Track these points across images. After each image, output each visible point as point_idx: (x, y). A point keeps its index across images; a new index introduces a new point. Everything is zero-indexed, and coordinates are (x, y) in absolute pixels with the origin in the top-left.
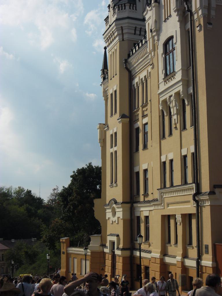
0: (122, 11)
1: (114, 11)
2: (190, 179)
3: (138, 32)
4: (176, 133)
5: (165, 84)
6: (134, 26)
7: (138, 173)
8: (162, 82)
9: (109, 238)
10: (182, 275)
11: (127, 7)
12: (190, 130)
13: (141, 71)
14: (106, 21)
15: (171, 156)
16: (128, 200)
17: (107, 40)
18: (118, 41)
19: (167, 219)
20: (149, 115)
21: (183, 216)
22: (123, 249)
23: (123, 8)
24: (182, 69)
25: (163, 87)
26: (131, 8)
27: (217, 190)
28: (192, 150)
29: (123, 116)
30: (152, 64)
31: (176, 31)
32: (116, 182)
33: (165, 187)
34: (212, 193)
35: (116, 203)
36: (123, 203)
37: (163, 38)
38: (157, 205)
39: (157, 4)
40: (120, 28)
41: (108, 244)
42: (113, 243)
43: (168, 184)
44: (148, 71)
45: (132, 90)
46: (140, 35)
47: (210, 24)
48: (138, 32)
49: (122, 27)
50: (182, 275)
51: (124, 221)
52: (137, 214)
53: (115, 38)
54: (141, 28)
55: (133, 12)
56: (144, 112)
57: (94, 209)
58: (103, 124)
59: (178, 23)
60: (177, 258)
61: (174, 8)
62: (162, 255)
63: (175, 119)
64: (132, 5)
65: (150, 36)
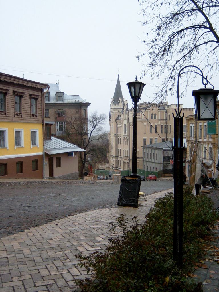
2: (128, 156)
4: (126, 145)
7: (119, 149)
11: (116, 105)
12: (128, 146)
15: (125, 150)
19: (124, 162)
29: (115, 135)
41: (111, 166)
42: (112, 166)
51: (115, 161)
52: (118, 159)
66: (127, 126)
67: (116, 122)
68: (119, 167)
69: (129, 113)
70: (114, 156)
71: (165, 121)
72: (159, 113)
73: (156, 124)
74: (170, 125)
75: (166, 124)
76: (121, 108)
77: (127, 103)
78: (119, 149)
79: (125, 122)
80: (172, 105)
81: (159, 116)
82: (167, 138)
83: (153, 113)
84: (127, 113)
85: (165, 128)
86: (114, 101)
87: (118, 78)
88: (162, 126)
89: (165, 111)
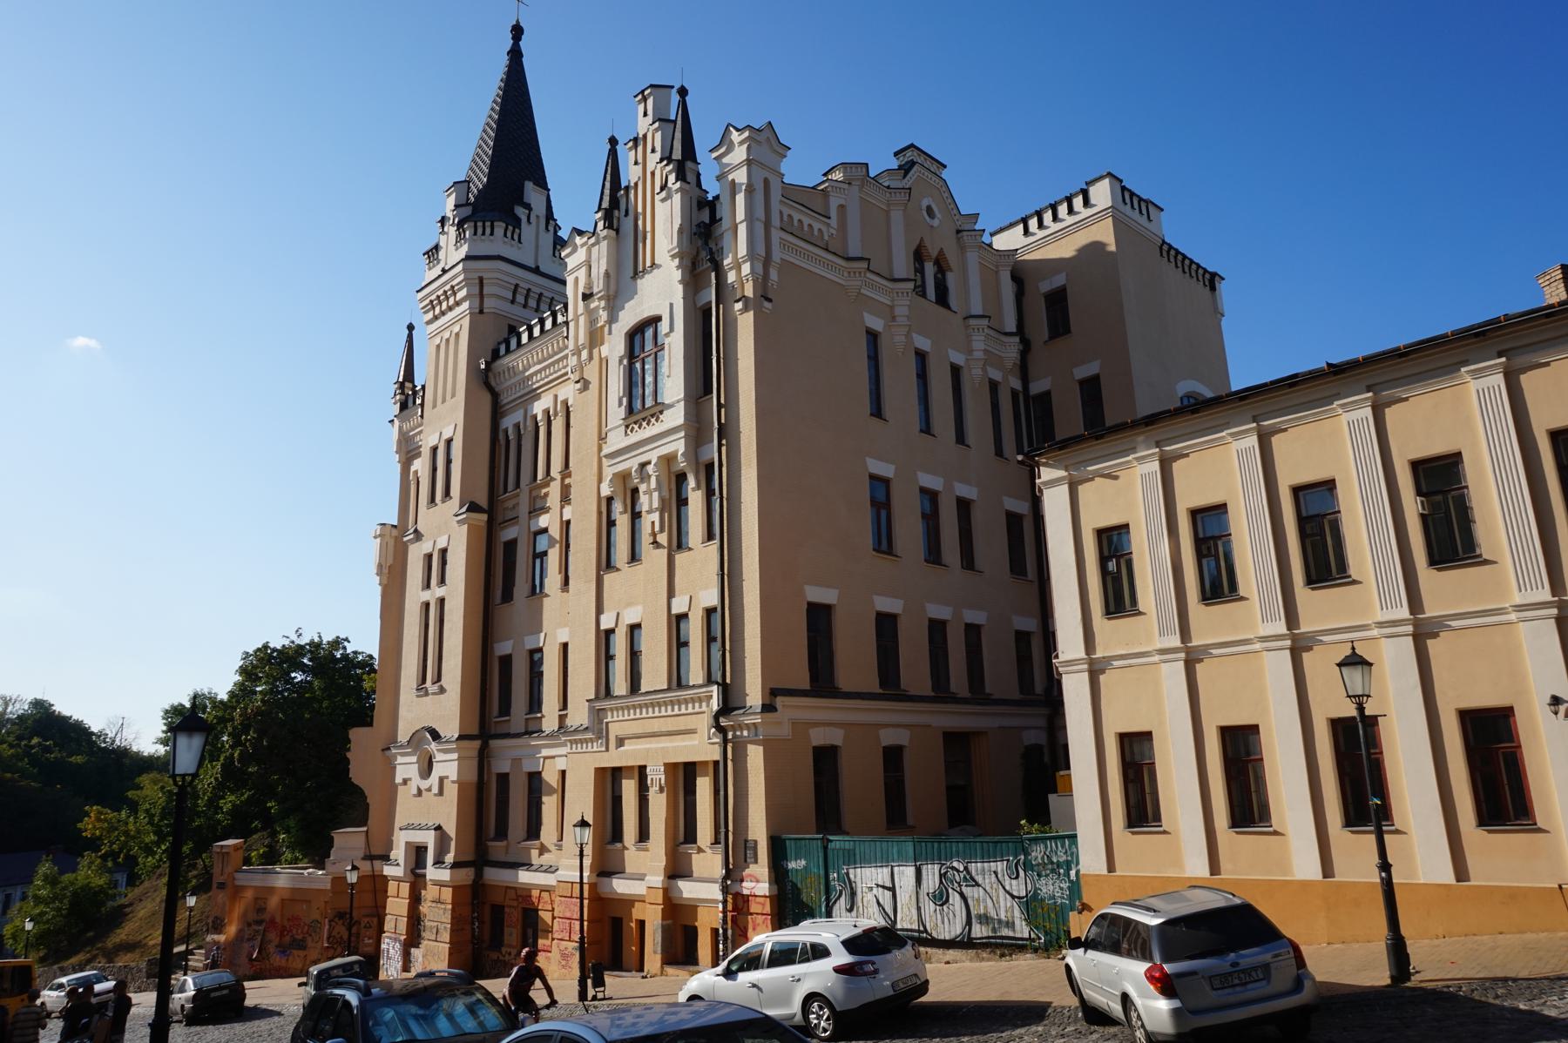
0: (483, 237)
1: (460, 234)
3: (520, 299)
5: (626, 432)
6: (514, 282)
8: (620, 426)
9: (401, 841)
10: (665, 923)
14: (429, 257)
16: (475, 731)
17: (430, 306)
18: (468, 312)
19: (610, 779)
21: (671, 768)
22: (456, 865)
23: (488, 231)
24: (687, 398)
25: (617, 440)
26: (509, 234)
28: (711, 598)
30: (582, 381)
31: (671, 305)
33: (608, 693)
34: (768, 708)
35: (435, 735)
36: (461, 738)
37: (629, 316)
38: (582, 744)
39: (613, 233)
40: (477, 281)
41: (399, 853)
43: (620, 686)
44: (556, 397)
45: (499, 441)
46: (525, 306)
48: (520, 299)
49: (481, 280)
50: (665, 923)
51: (462, 785)
53: (457, 304)
54: (529, 290)
55: (512, 246)
56: (534, 500)
57: (349, 755)
58: (393, 526)
59: (680, 287)
60: (647, 878)
61: (672, 250)
62: (595, 875)
63: (653, 523)
64: (510, 228)
65: (581, 309)
71: (1011, 351)
73: (958, 358)
76: (536, 270)
77: (683, 92)
80: (1092, 191)
83: (927, 243)
86: (468, 211)
87: (515, 55)
88: (994, 386)
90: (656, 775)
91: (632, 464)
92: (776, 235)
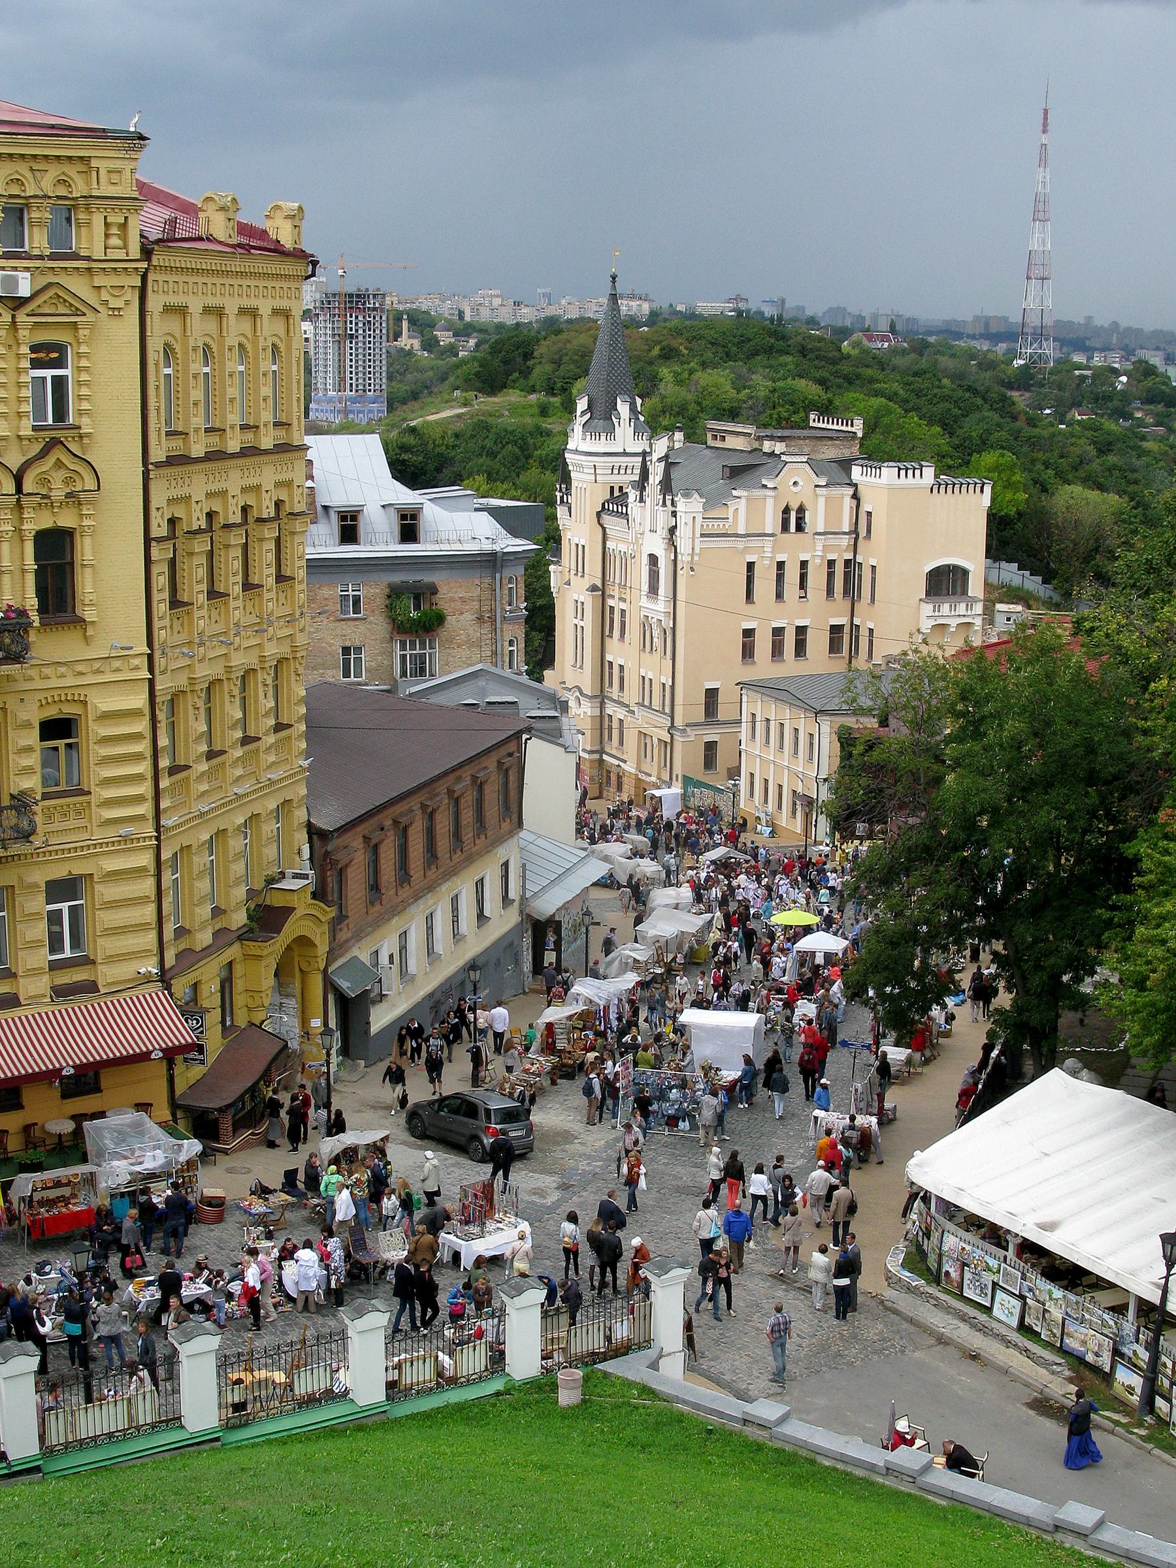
2: (667, 710)
3: (616, 471)
4: (657, 656)
7: (611, 663)
13: (618, 540)
15: (650, 675)
20: (628, 601)
27: (688, 729)
29: (594, 588)
32: (581, 667)
35: (581, 693)
43: (647, 703)
47: (692, 569)
48: (616, 471)
66: (662, 563)
67: (601, 526)
68: (614, 752)
69: (673, 504)
70: (588, 691)
71: (846, 541)
72: (821, 502)
73: (804, 557)
74: (873, 562)
75: (850, 556)
76: (625, 454)
78: (611, 663)
79: (656, 545)
81: (816, 520)
82: (856, 621)
84: (664, 504)
85: (847, 575)
86: (588, 416)
88: (831, 563)
89: (851, 491)
90: (655, 741)
91: (650, 615)
92: (697, 541)
